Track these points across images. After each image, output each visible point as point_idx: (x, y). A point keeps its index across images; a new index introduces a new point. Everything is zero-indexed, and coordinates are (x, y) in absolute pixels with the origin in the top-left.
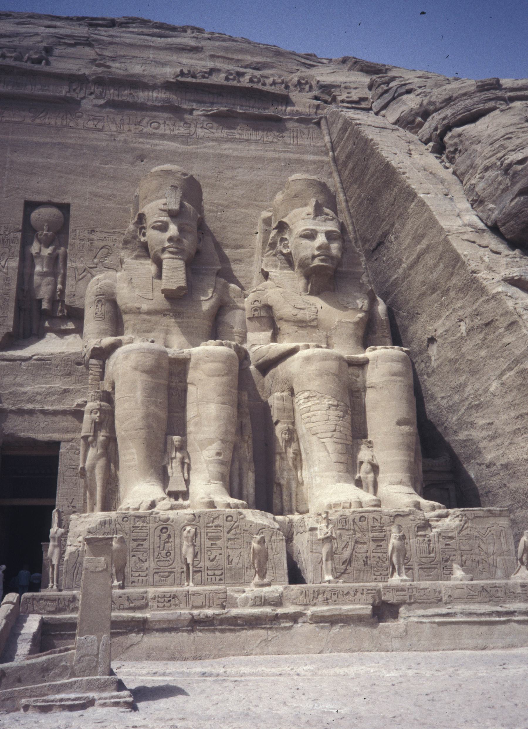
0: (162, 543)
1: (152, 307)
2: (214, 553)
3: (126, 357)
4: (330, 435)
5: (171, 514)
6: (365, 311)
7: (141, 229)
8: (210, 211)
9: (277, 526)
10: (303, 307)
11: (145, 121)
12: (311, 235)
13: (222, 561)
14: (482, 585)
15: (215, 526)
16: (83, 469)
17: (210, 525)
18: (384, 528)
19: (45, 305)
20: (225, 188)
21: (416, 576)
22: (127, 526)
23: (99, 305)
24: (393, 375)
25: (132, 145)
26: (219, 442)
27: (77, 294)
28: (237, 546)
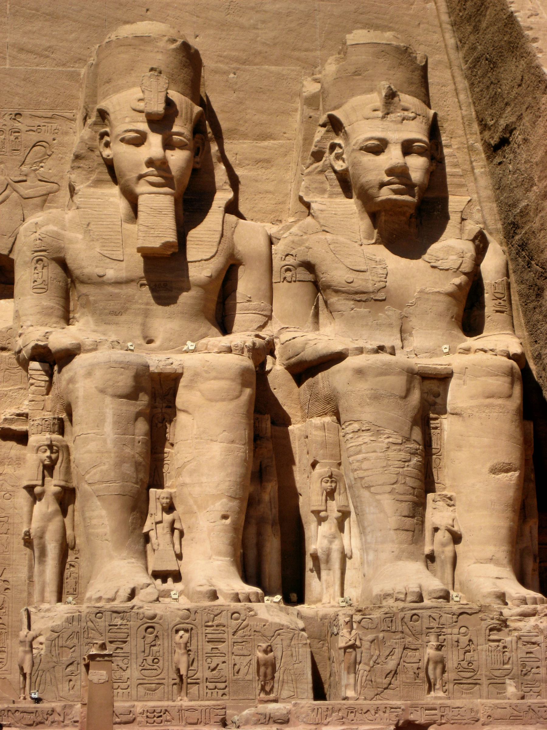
0: (147, 647)
1: (124, 275)
2: (215, 661)
3: (89, 374)
4: (388, 488)
5: (158, 609)
6: (465, 274)
8: (216, 71)
9: (301, 624)
10: (363, 268)
12: (378, 148)
13: (226, 670)
14: (529, 704)
15: (217, 626)
16: (28, 534)
17: (210, 624)
18: (444, 630)
20: (242, 28)
21: (485, 694)
22: (102, 623)
23: (39, 266)
24: (488, 397)
26: (225, 500)
28: (245, 652)
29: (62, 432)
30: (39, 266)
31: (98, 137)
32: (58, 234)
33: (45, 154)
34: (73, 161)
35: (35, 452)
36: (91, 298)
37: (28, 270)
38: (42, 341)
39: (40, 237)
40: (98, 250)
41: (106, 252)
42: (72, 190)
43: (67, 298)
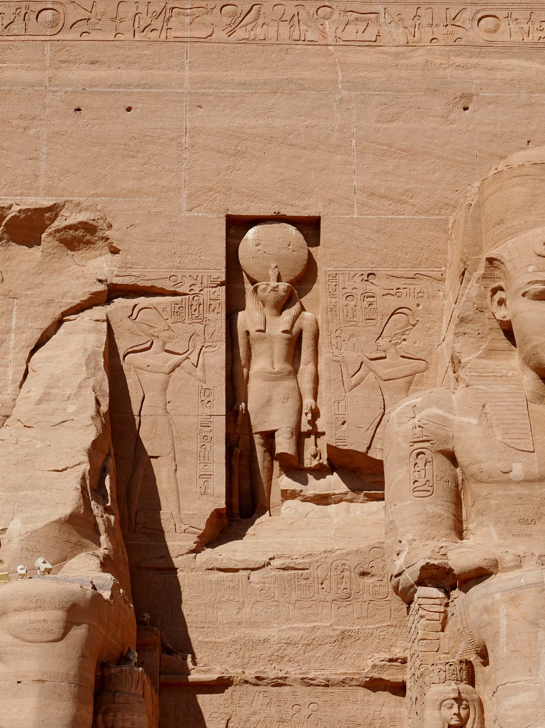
1: (536, 470)
7: (494, 291)
11: (467, 15)
19: (284, 445)
25: (441, 73)
27: (348, 420)
29: (471, 681)
30: (421, 461)
31: (490, 294)
32: (445, 420)
33: (409, 323)
34: (457, 326)
35: (437, 708)
36: (493, 502)
37: (405, 468)
38: (435, 559)
39: (420, 424)
40: (499, 438)
41: (509, 441)
42: (456, 363)
43: (458, 503)
